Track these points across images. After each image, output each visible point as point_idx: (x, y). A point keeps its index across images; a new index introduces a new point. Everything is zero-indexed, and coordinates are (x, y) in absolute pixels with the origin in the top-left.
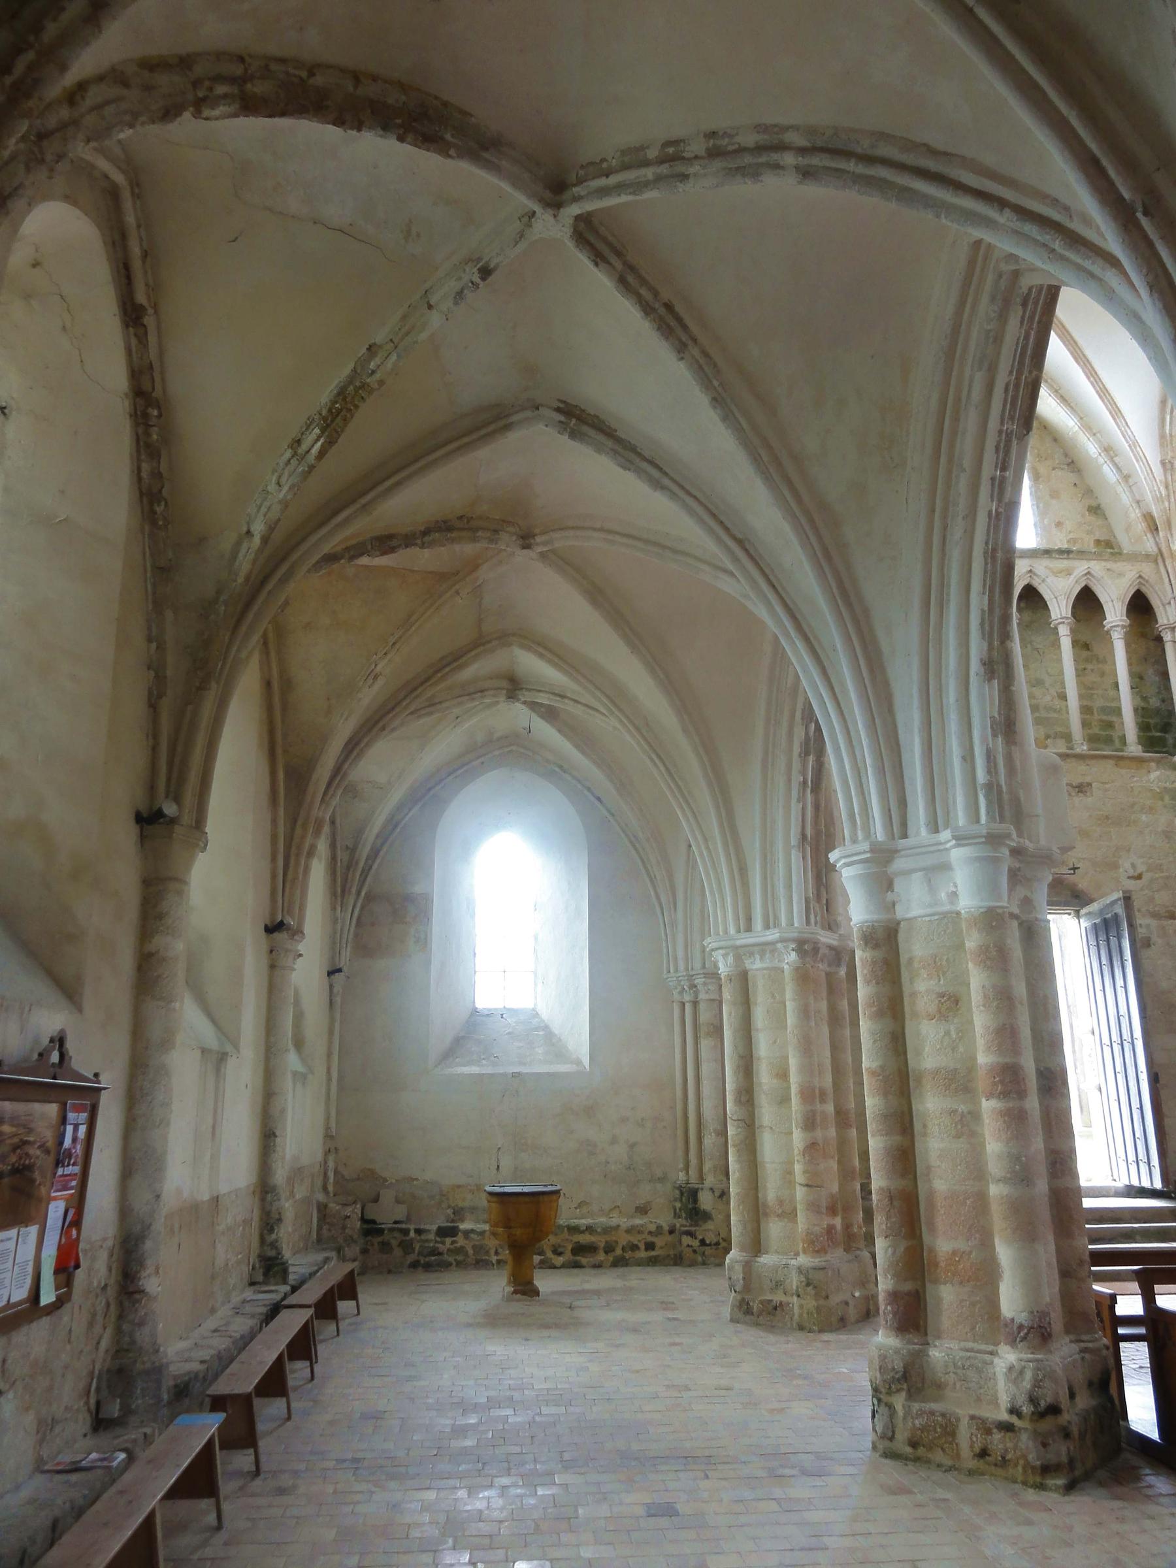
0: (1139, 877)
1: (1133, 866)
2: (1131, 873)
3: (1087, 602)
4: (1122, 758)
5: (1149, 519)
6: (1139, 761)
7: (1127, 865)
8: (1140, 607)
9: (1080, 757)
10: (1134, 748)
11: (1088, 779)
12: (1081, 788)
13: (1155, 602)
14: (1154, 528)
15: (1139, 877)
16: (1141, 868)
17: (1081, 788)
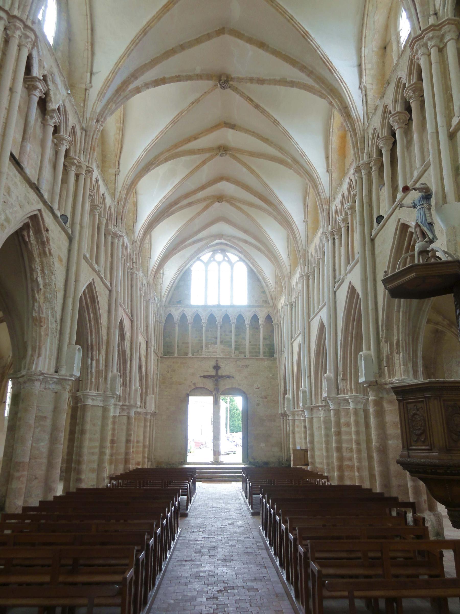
0: (259, 388)
1: (258, 386)
2: (257, 387)
3: (255, 318)
4: (257, 359)
5: (271, 296)
6: (262, 359)
7: (256, 386)
8: (269, 318)
9: (247, 359)
10: (261, 356)
11: (249, 364)
12: (246, 366)
13: (273, 318)
14: (272, 299)
15: (259, 388)
16: (259, 386)
17: (246, 366)
